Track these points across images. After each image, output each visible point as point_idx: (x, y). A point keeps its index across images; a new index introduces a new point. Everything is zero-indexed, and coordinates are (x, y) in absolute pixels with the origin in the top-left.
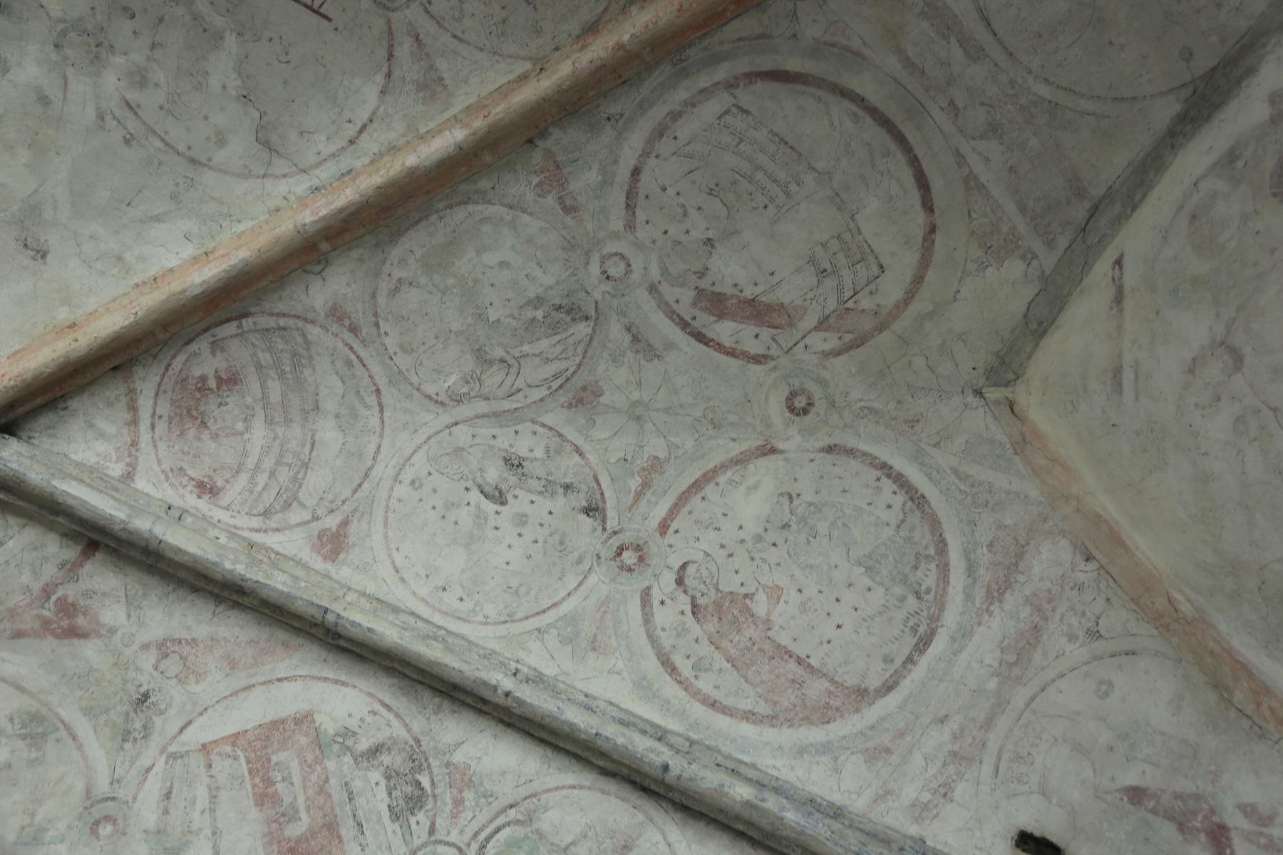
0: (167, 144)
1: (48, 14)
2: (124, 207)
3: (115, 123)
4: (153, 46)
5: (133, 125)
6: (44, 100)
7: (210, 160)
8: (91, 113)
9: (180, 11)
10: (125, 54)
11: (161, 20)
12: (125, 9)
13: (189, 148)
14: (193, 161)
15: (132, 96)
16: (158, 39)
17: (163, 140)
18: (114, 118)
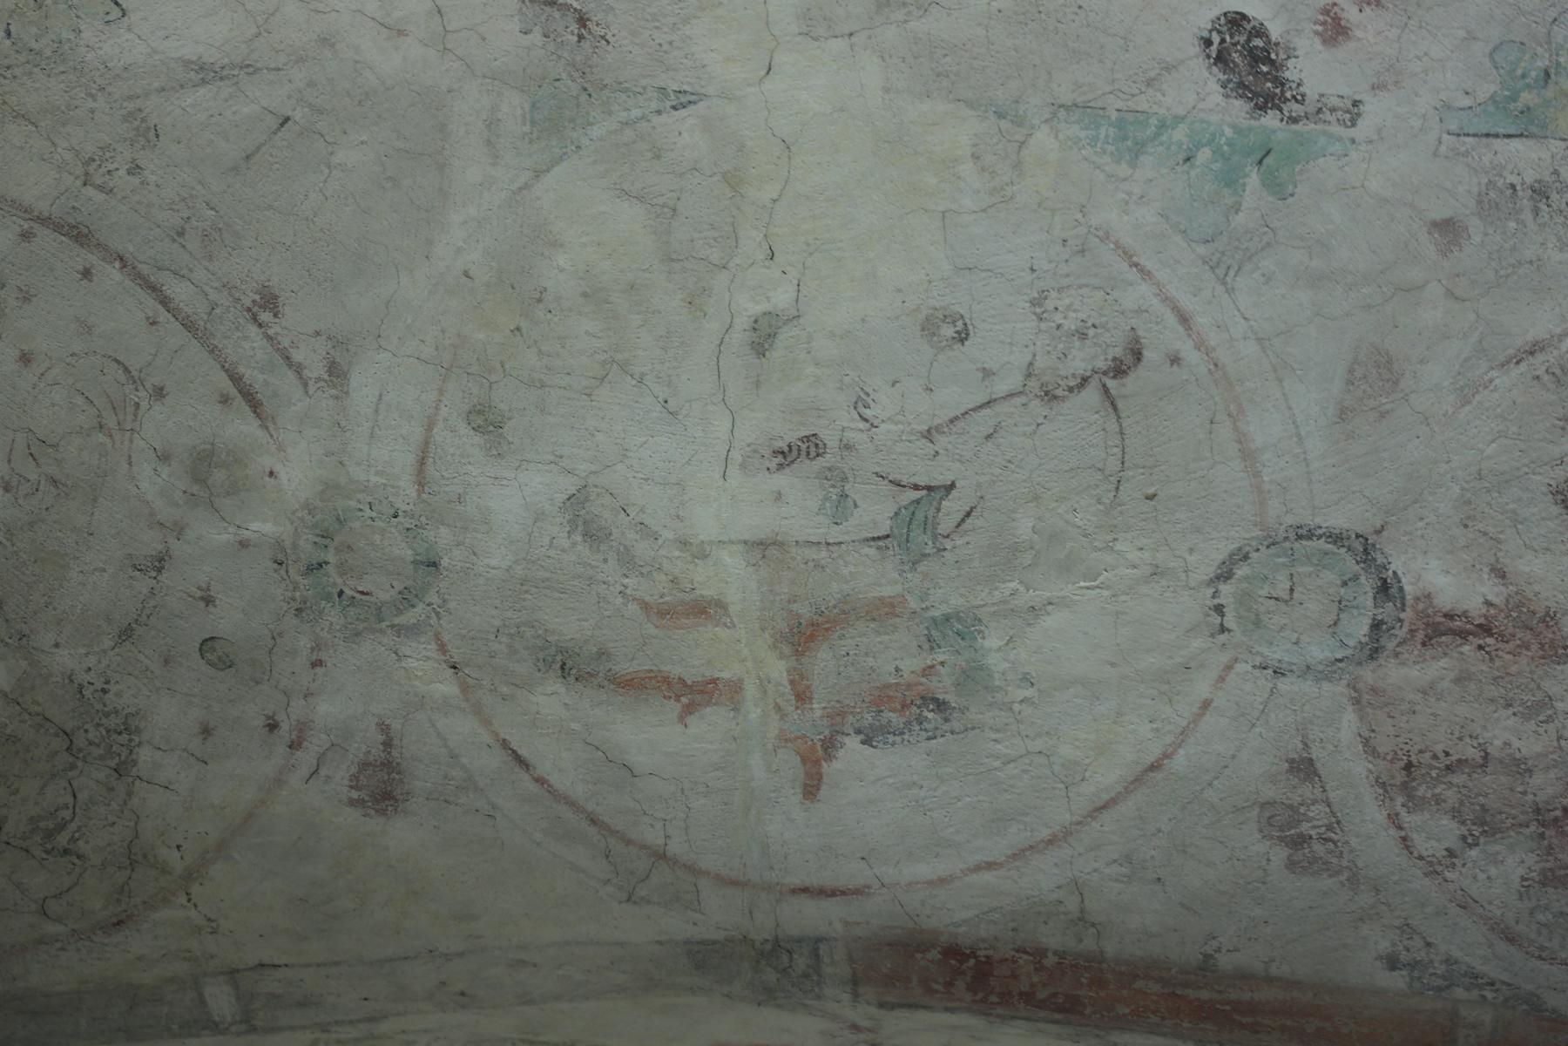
0: (153, 288)
1: (442, 648)
2: (297, 115)
3: (297, 356)
4: (160, 563)
5: (249, 350)
6: (487, 422)
7: (26, 236)
8: (363, 385)
9: (65, 659)
10: (244, 544)
11: (126, 634)
12: (226, 664)
13: (87, 273)
14: (80, 235)
15: (242, 426)
16: (143, 584)
17: (165, 302)
18: (298, 369)
